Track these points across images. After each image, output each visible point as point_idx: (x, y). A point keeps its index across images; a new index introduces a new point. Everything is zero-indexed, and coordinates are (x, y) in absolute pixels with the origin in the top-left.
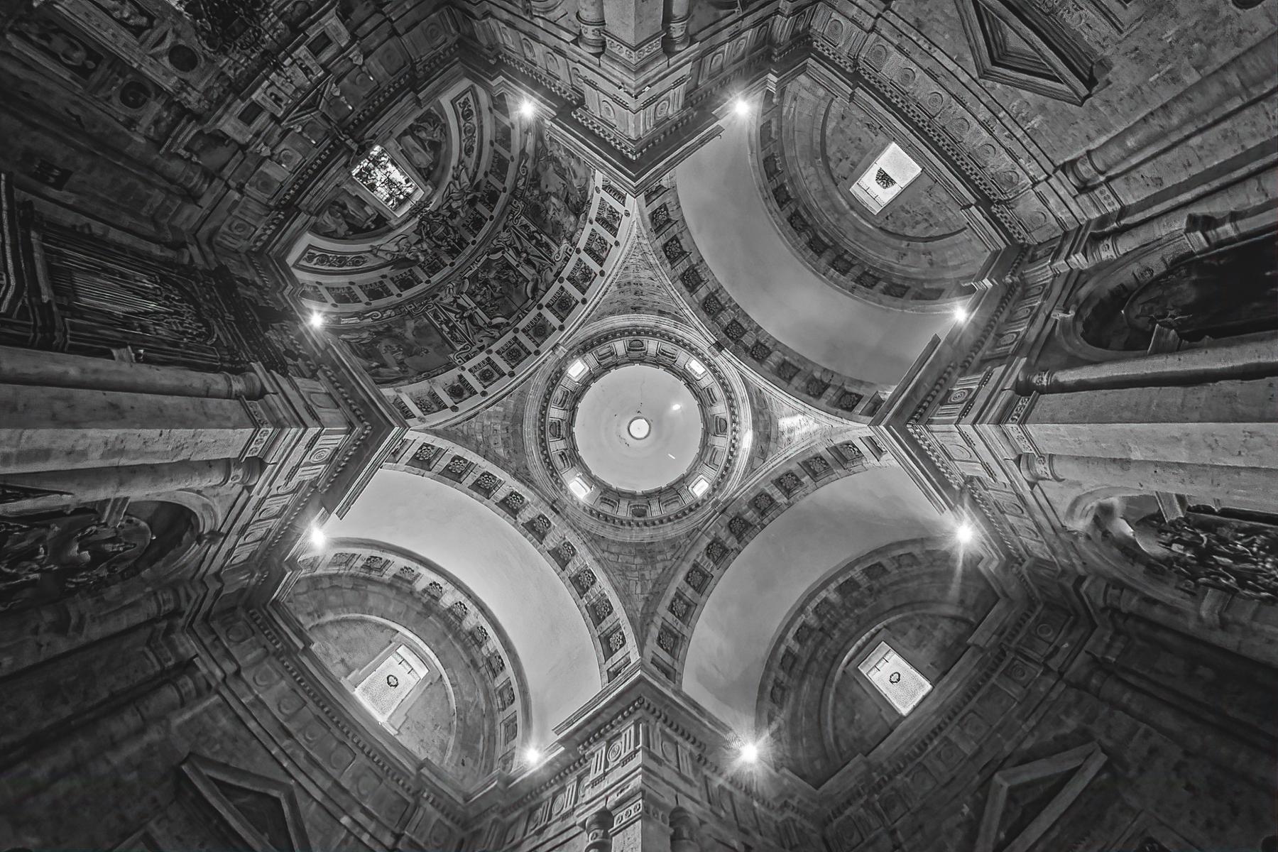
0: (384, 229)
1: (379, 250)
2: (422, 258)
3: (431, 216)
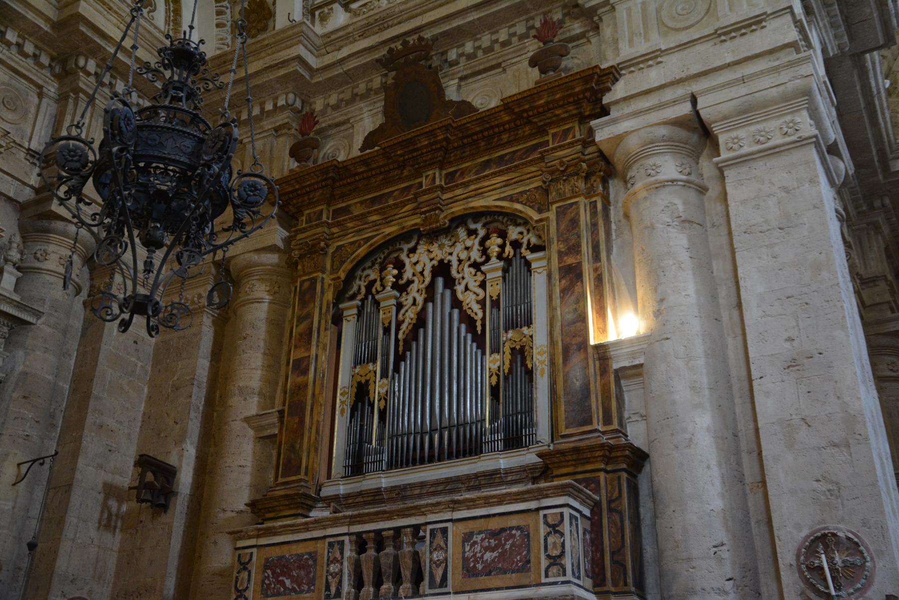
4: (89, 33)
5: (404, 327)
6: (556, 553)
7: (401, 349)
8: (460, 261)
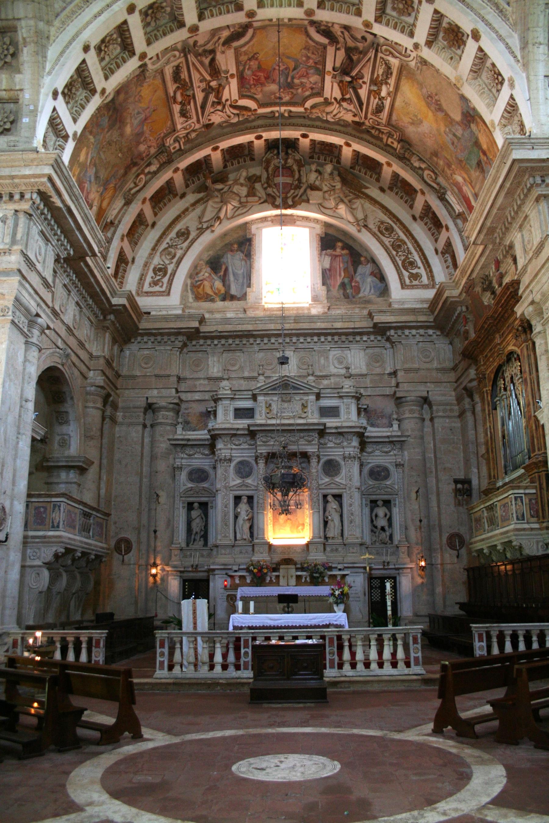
0: (330, 232)
1: (357, 221)
2: (329, 168)
3: (279, 201)
4: (383, 325)
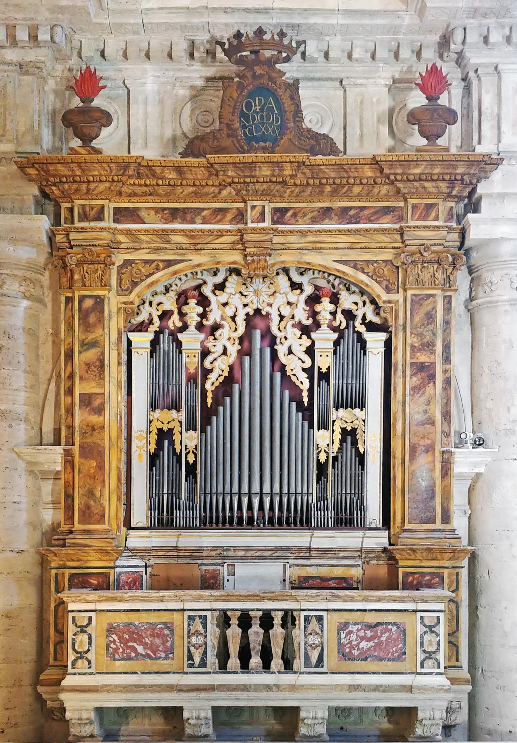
5: (212, 377)
6: (433, 649)
7: (209, 401)
8: (282, 317)
